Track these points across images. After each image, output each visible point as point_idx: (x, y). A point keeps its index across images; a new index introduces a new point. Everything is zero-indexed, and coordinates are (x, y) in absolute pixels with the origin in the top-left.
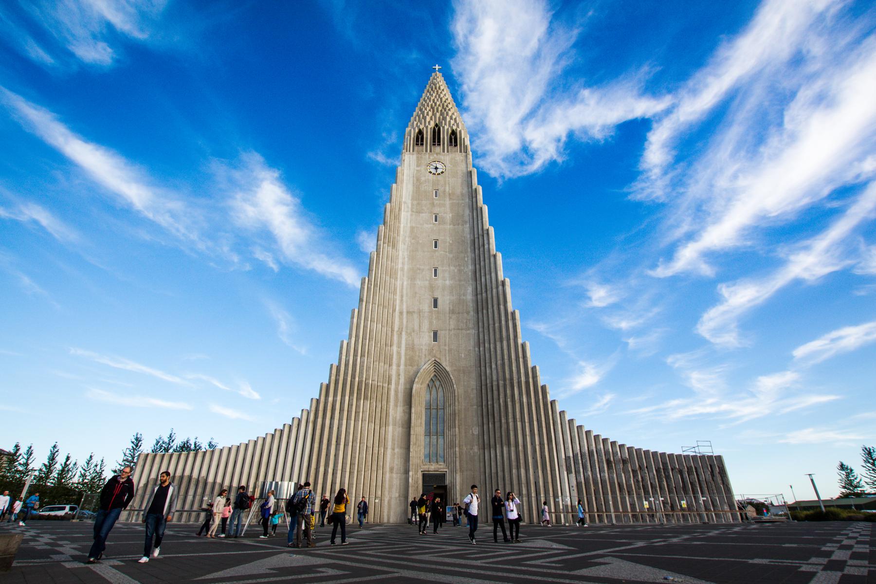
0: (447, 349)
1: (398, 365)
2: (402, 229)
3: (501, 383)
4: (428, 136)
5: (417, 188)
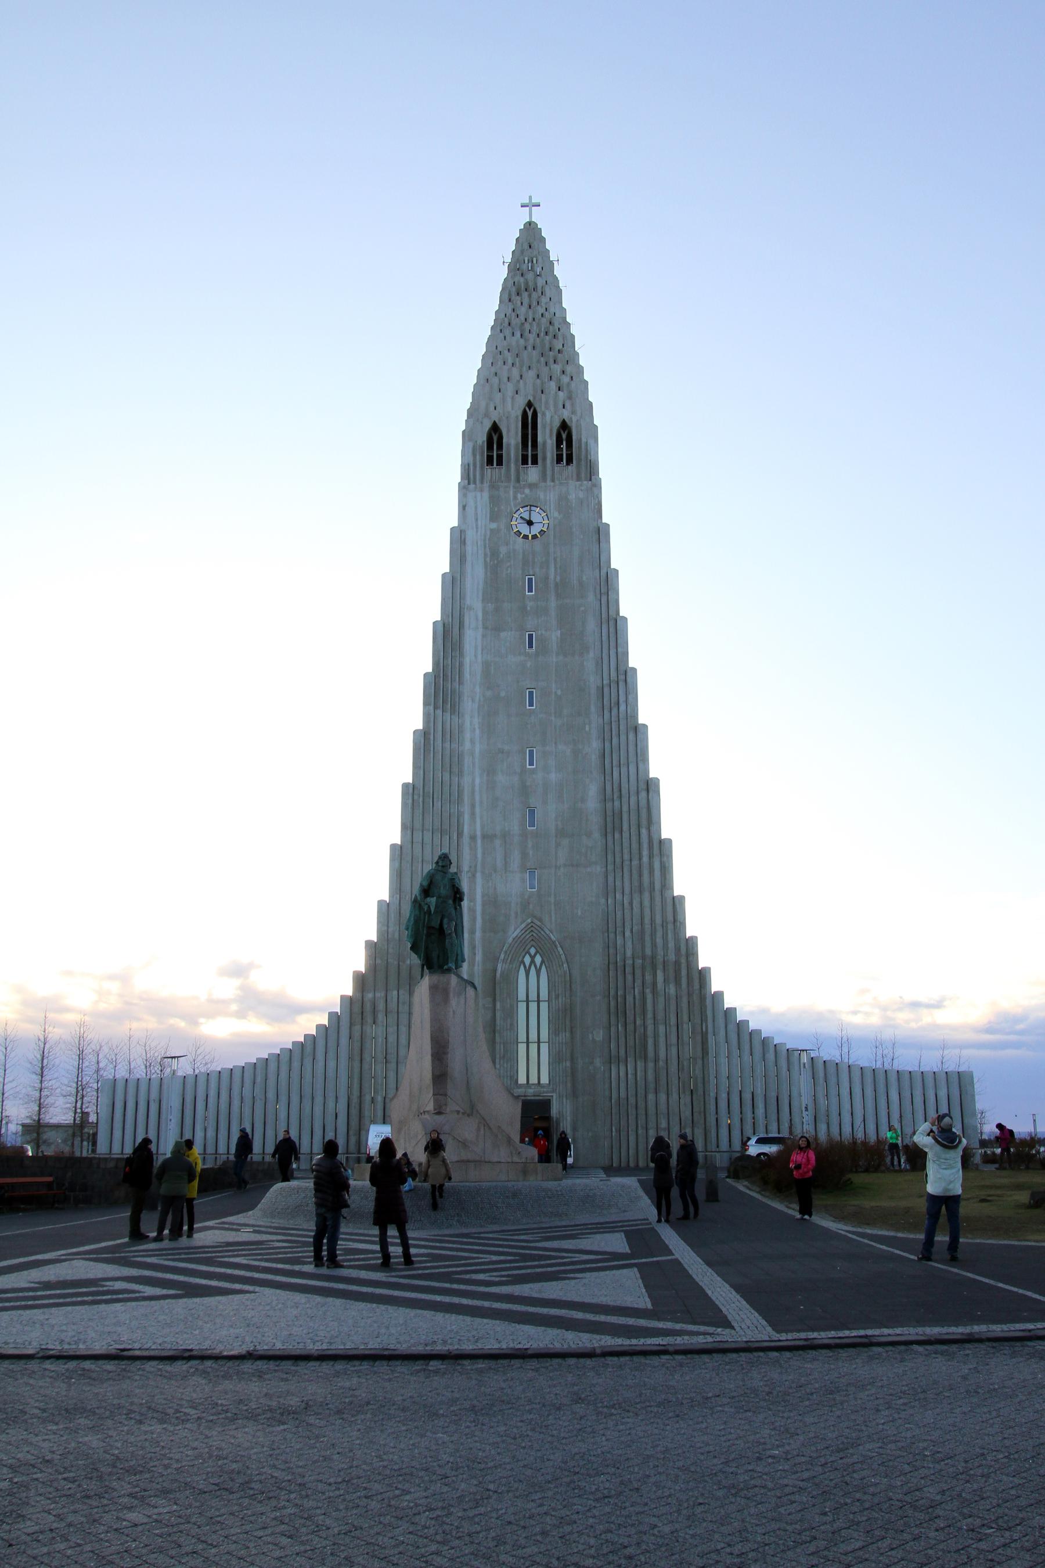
0: (553, 901)
1: (472, 932)
4: (512, 438)
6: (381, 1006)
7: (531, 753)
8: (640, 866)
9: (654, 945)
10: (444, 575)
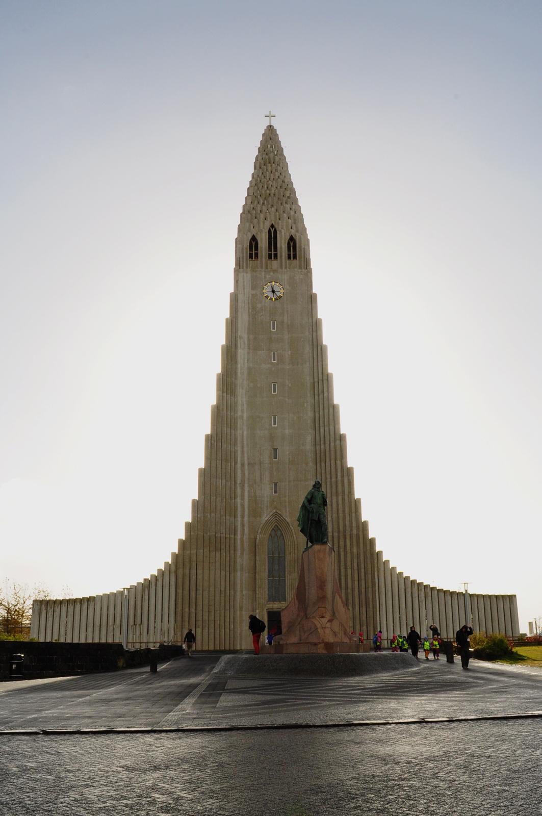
0: (287, 500)
1: (243, 517)
2: (239, 371)
3: (336, 534)
4: (263, 243)
5: (252, 318)
6: (194, 558)
7: (275, 418)
8: (336, 482)
9: (345, 526)
10: (227, 320)
